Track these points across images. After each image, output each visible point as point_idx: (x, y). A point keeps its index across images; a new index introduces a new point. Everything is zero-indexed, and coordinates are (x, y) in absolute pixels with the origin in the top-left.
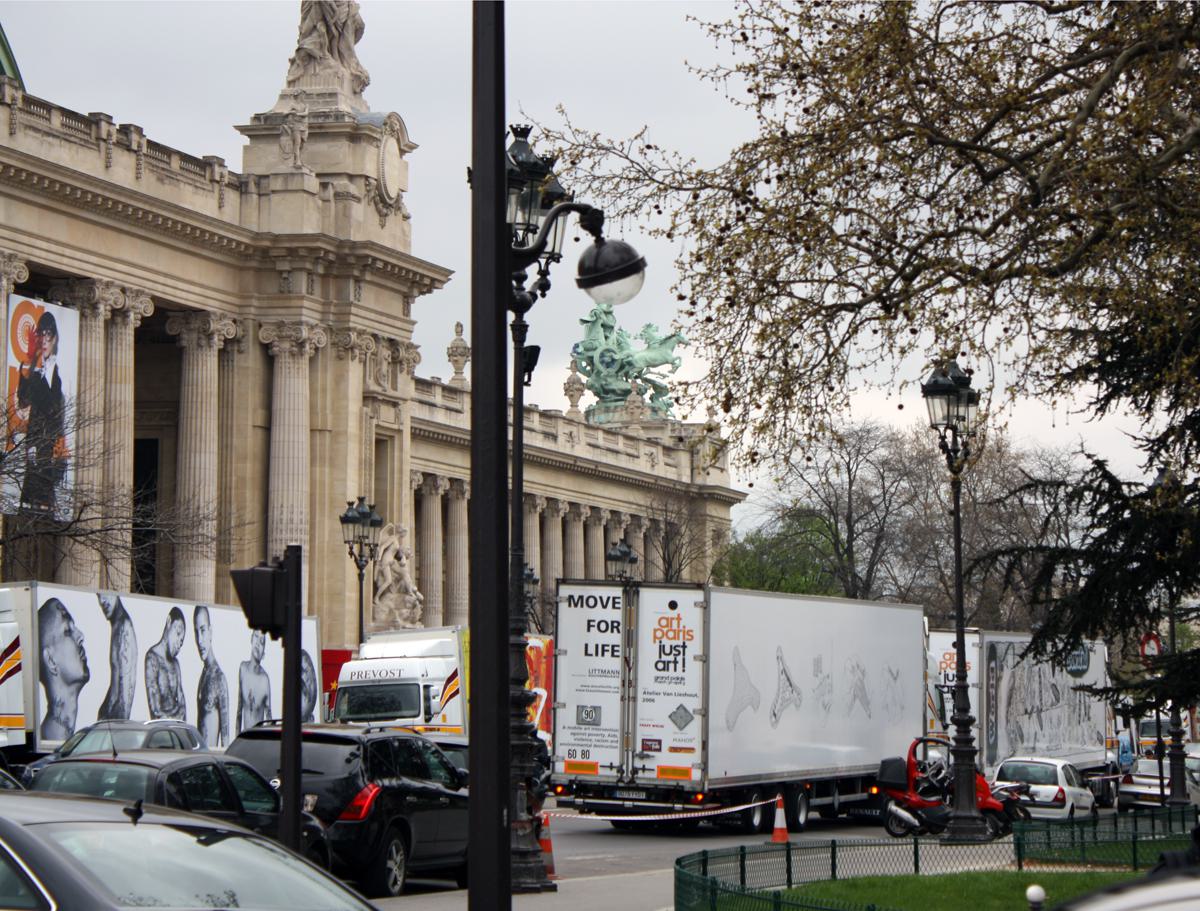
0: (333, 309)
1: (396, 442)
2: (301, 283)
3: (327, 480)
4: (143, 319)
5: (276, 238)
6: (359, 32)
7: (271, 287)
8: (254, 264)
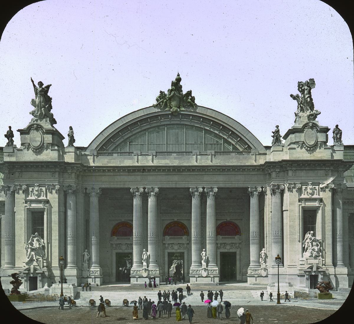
2: (274, 175)
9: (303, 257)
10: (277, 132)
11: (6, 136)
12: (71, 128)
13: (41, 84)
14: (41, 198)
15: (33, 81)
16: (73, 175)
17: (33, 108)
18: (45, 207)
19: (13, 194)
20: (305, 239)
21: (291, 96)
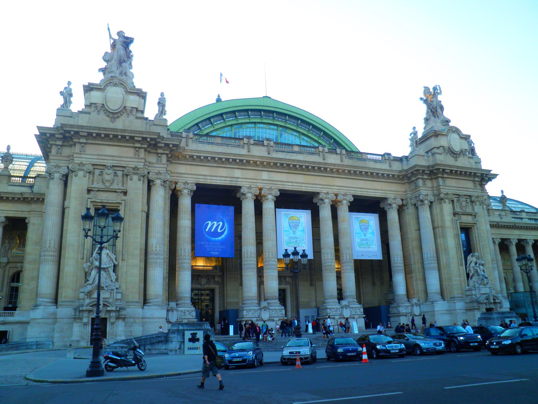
0: (435, 189)
1: (475, 227)
2: (420, 182)
3: (442, 242)
4: (351, 202)
5: (407, 171)
6: (442, 108)
7: (413, 187)
8: (406, 181)
9: (468, 286)
10: (415, 133)
11: (61, 93)
12: (162, 94)
13: (120, 34)
14: (115, 187)
15: (109, 29)
16: (164, 158)
17: (104, 64)
18: (121, 202)
19: (64, 179)
20: (468, 263)
21: (421, 99)
